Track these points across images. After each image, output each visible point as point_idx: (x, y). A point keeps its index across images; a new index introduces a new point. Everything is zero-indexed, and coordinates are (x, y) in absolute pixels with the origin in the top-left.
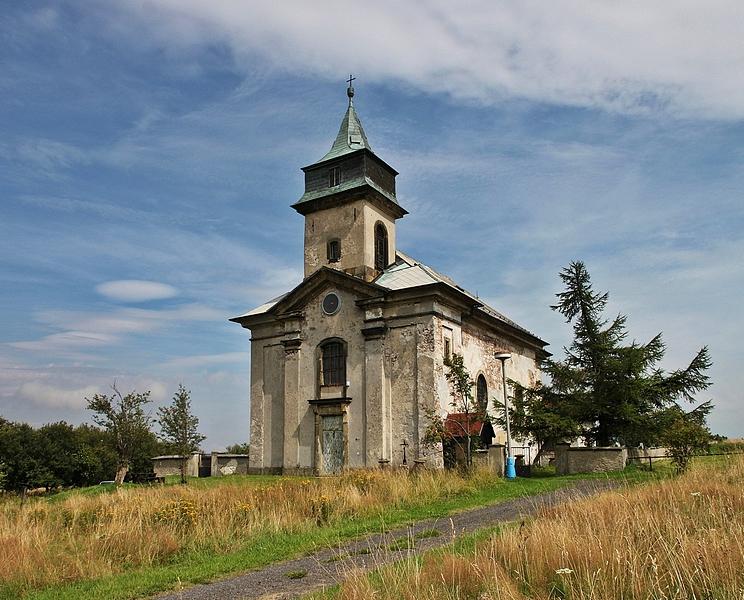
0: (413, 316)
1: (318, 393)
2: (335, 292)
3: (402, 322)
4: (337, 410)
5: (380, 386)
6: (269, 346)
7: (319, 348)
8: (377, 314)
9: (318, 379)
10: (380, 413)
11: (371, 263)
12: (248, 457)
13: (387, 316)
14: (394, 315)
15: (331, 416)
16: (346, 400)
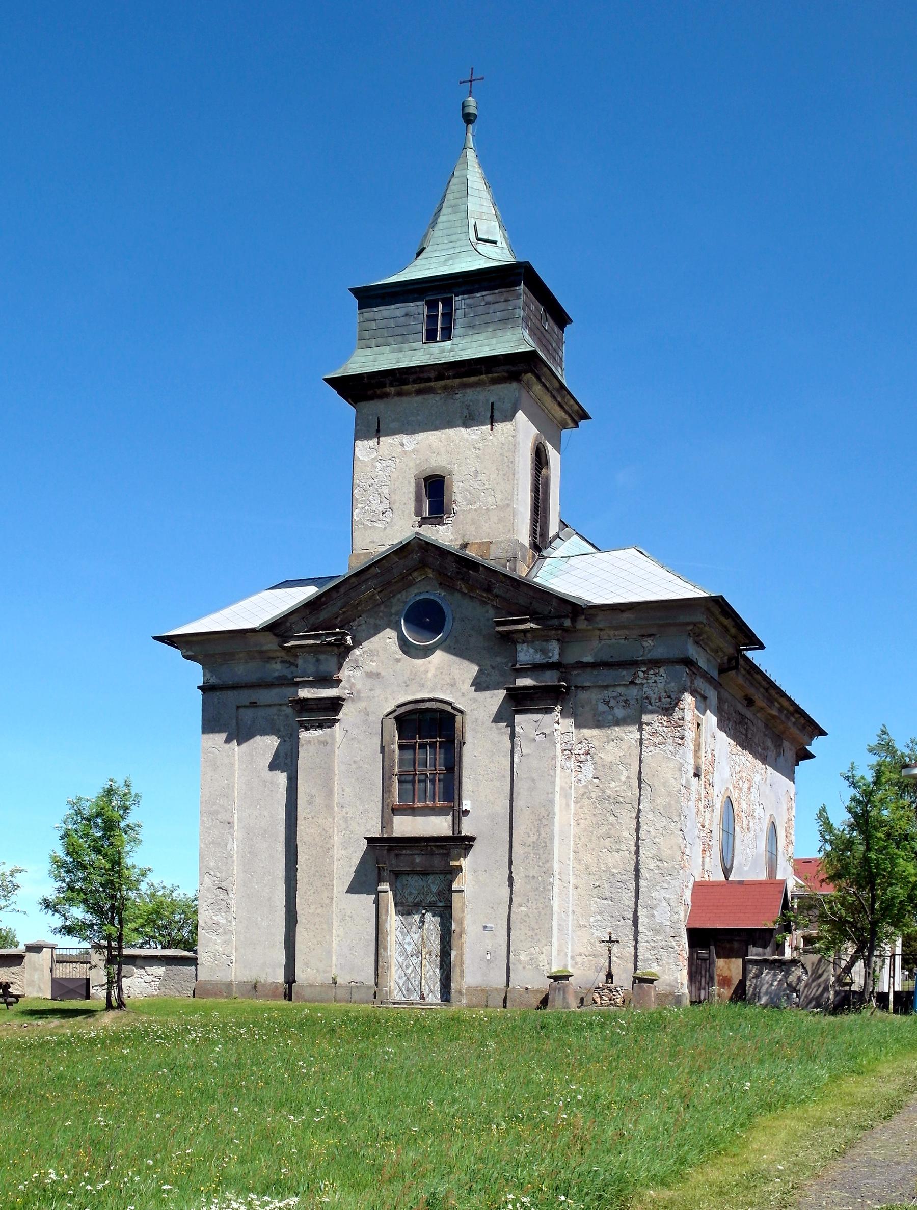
0: (633, 664)
1: (386, 823)
2: (438, 595)
3: (606, 676)
4: (437, 862)
5: (550, 815)
6: (253, 705)
7: (391, 724)
8: (544, 652)
9: (386, 790)
10: (549, 873)
11: (524, 537)
12: (193, 962)
13: (570, 659)
14: (588, 659)
15: (418, 873)
16: (463, 843)
